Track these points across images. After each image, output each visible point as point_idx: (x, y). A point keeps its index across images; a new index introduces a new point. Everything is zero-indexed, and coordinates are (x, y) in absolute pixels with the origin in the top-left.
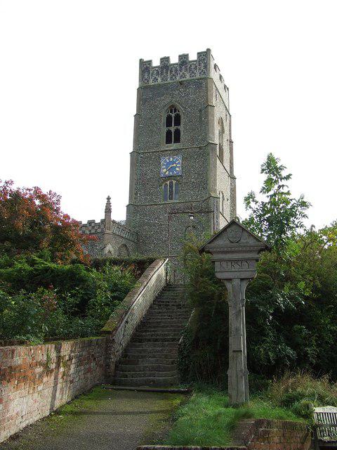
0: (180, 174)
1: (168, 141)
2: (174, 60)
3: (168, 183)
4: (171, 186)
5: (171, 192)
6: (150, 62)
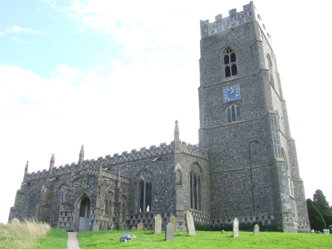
0: (240, 99)
1: (228, 75)
2: (226, 15)
3: (230, 107)
4: (233, 110)
5: (234, 114)
6: (207, 21)
